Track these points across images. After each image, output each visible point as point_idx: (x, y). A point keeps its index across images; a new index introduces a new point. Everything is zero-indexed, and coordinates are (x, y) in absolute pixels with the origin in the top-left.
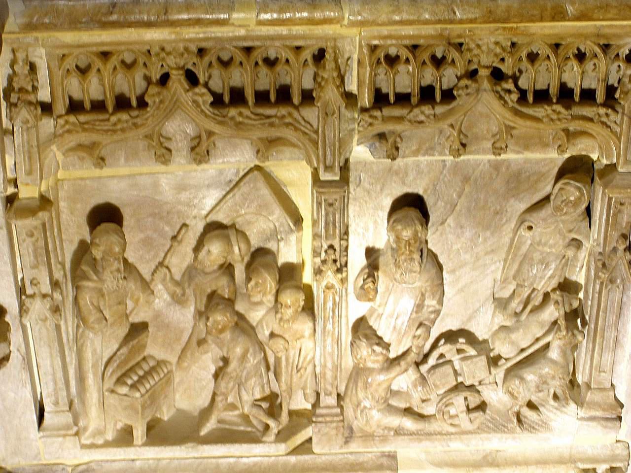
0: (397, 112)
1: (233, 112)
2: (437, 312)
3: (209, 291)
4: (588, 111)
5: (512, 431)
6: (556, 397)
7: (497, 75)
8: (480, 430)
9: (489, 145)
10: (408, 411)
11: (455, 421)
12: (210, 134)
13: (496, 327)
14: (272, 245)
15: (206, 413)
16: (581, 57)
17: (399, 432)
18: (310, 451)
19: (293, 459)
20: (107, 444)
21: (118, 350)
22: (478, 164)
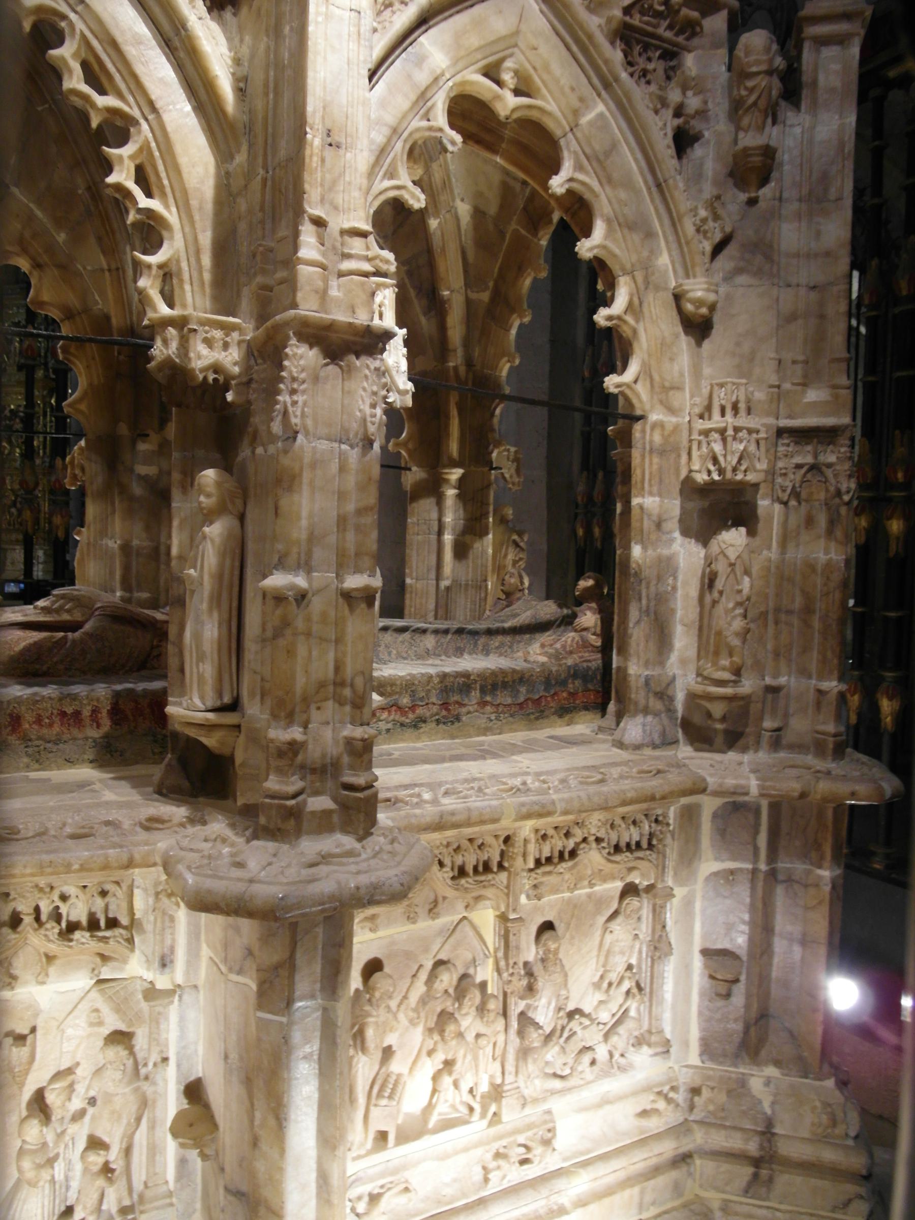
0: (548, 868)
1: (463, 881)
2: (567, 998)
3: (439, 1010)
4: (640, 854)
5: (614, 1075)
6: (633, 1045)
7: (598, 840)
8: (598, 1078)
9: (586, 883)
10: (555, 1075)
11: (583, 1076)
12: (444, 898)
13: (595, 1003)
14: (471, 971)
15: (429, 1108)
16: (634, 823)
17: (553, 1092)
18: (500, 1122)
19: (493, 1131)
20: (369, 1153)
21: (380, 1069)
22: (580, 896)
